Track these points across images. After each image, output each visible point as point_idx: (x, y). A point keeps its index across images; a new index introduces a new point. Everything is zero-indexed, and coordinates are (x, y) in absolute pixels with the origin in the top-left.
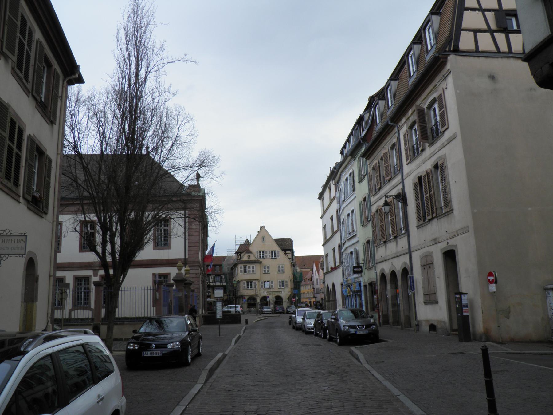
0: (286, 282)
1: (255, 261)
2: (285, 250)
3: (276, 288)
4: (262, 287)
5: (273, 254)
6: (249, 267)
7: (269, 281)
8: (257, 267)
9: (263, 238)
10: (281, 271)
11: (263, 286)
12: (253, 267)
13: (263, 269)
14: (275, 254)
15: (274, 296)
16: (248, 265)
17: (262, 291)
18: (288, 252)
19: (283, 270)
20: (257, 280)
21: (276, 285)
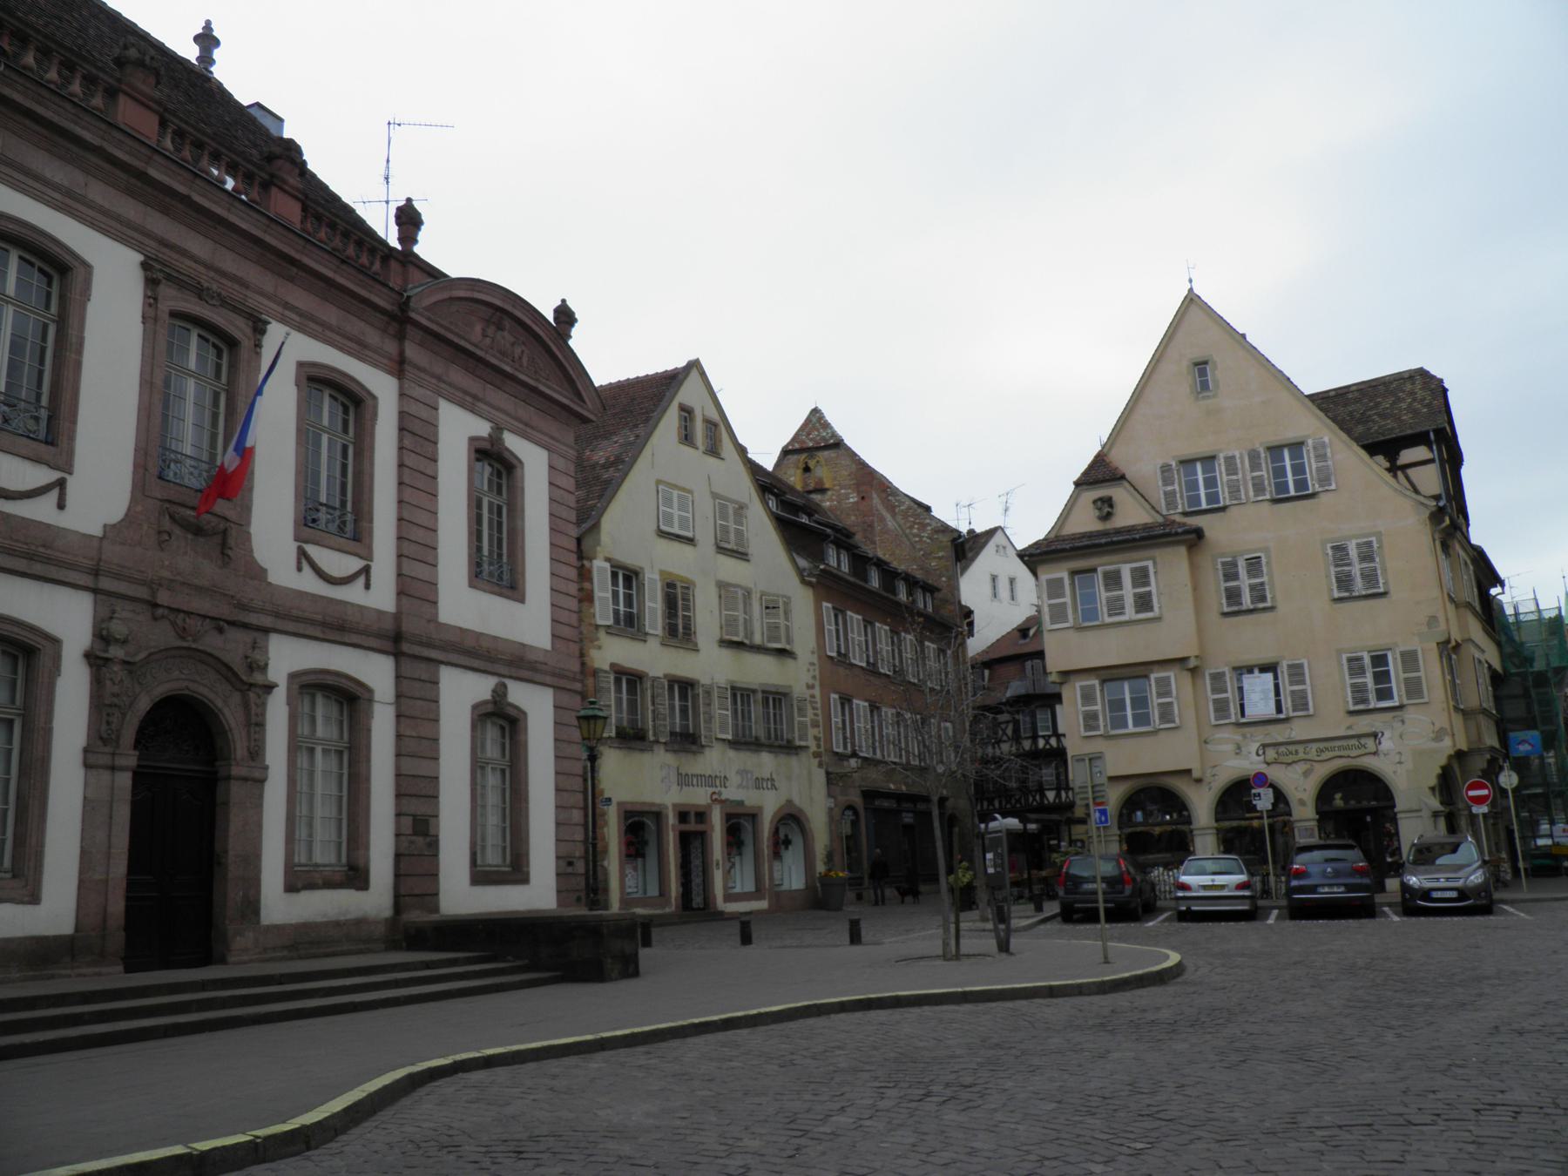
0: (1409, 659)
1: (1146, 527)
2: (1386, 448)
3: (1329, 715)
4: (1221, 708)
5: (1287, 479)
6: (1113, 580)
7: (1269, 668)
8: (1169, 571)
9: (1201, 366)
10: (1357, 579)
11: (1231, 712)
12: (1141, 577)
13: (1215, 587)
14: (1299, 469)
15: (1323, 771)
16: (1103, 564)
17: (1225, 740)
18: (1408, 455)
19: (1370, 577)
20: (1182, 661)
21: (1330, 692)
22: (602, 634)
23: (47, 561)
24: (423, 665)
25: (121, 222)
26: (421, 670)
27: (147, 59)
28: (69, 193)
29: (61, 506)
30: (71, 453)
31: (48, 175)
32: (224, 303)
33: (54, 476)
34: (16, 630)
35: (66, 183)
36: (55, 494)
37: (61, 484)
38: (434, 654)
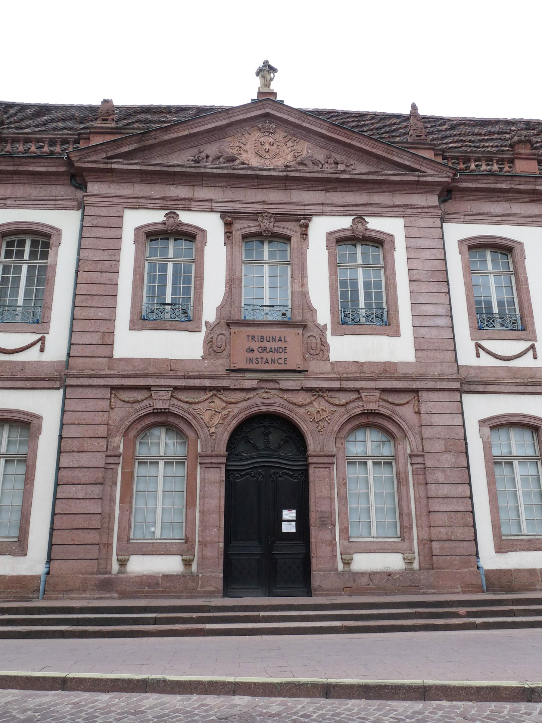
23: (534, 384)
25: (531, 217)
27: (523, 138)
28: (503, 215)
29: (535, 357)
30: (534, 331)
31: (493, 211)
33: (529, 344)
34: (527, 419)
35: (501, 211)
36: (531, 352)
37: (533, 347)
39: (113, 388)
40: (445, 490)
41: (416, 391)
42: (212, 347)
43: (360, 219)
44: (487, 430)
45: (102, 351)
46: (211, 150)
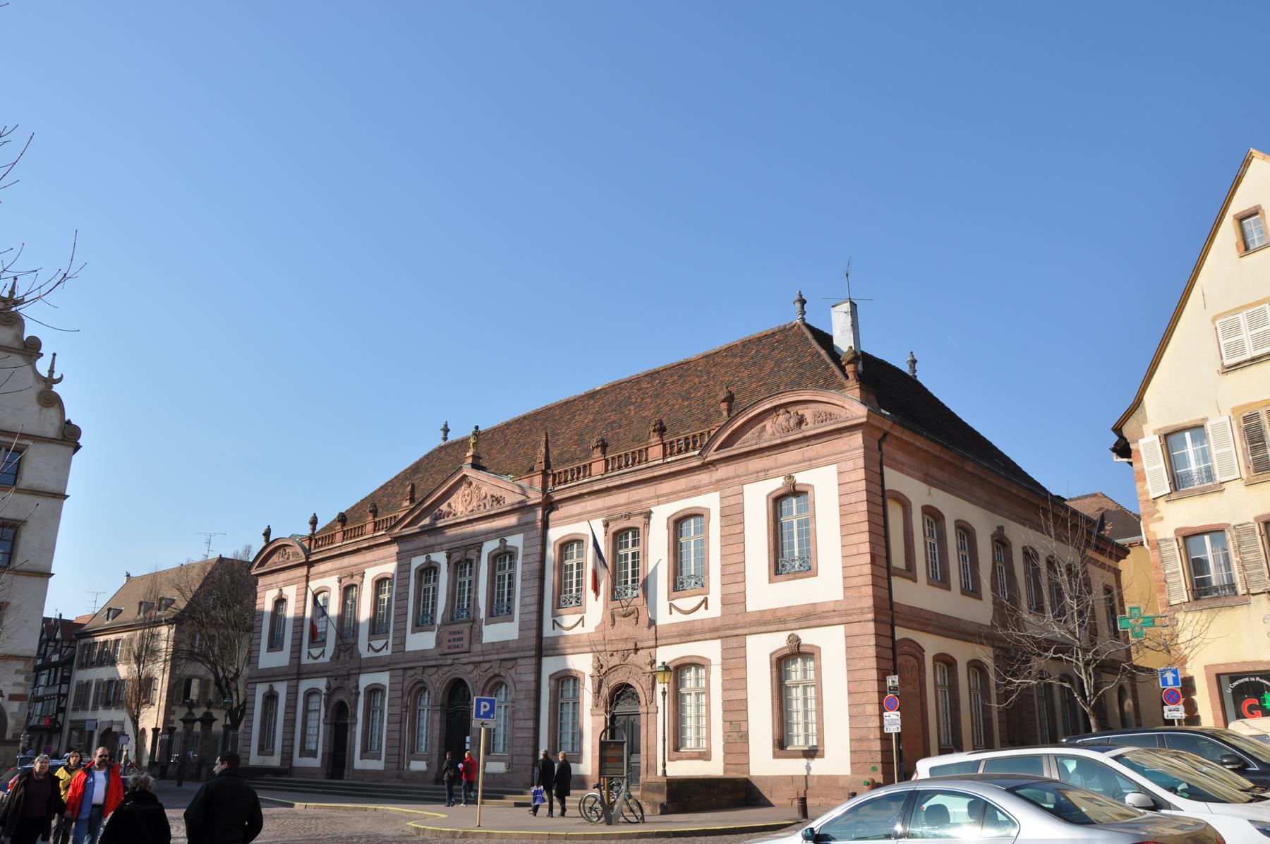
22: (1161, 503)
24: (734, 639)
26: (733, 642)
32: (628, 516)
37: (582, 619)
38: (739, 632)
39: (405, 669)
40: (522, 724)
41: (515, 659)
42: (439, 641)
43: (503, 541)
44: (553, 682)
45: (401, 647)
46: (444, 507)
